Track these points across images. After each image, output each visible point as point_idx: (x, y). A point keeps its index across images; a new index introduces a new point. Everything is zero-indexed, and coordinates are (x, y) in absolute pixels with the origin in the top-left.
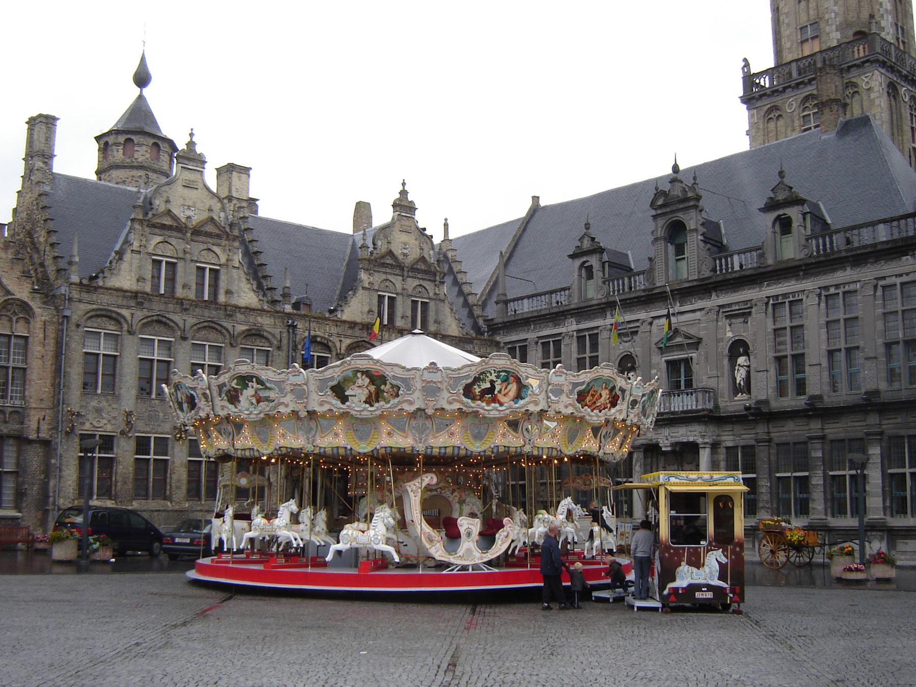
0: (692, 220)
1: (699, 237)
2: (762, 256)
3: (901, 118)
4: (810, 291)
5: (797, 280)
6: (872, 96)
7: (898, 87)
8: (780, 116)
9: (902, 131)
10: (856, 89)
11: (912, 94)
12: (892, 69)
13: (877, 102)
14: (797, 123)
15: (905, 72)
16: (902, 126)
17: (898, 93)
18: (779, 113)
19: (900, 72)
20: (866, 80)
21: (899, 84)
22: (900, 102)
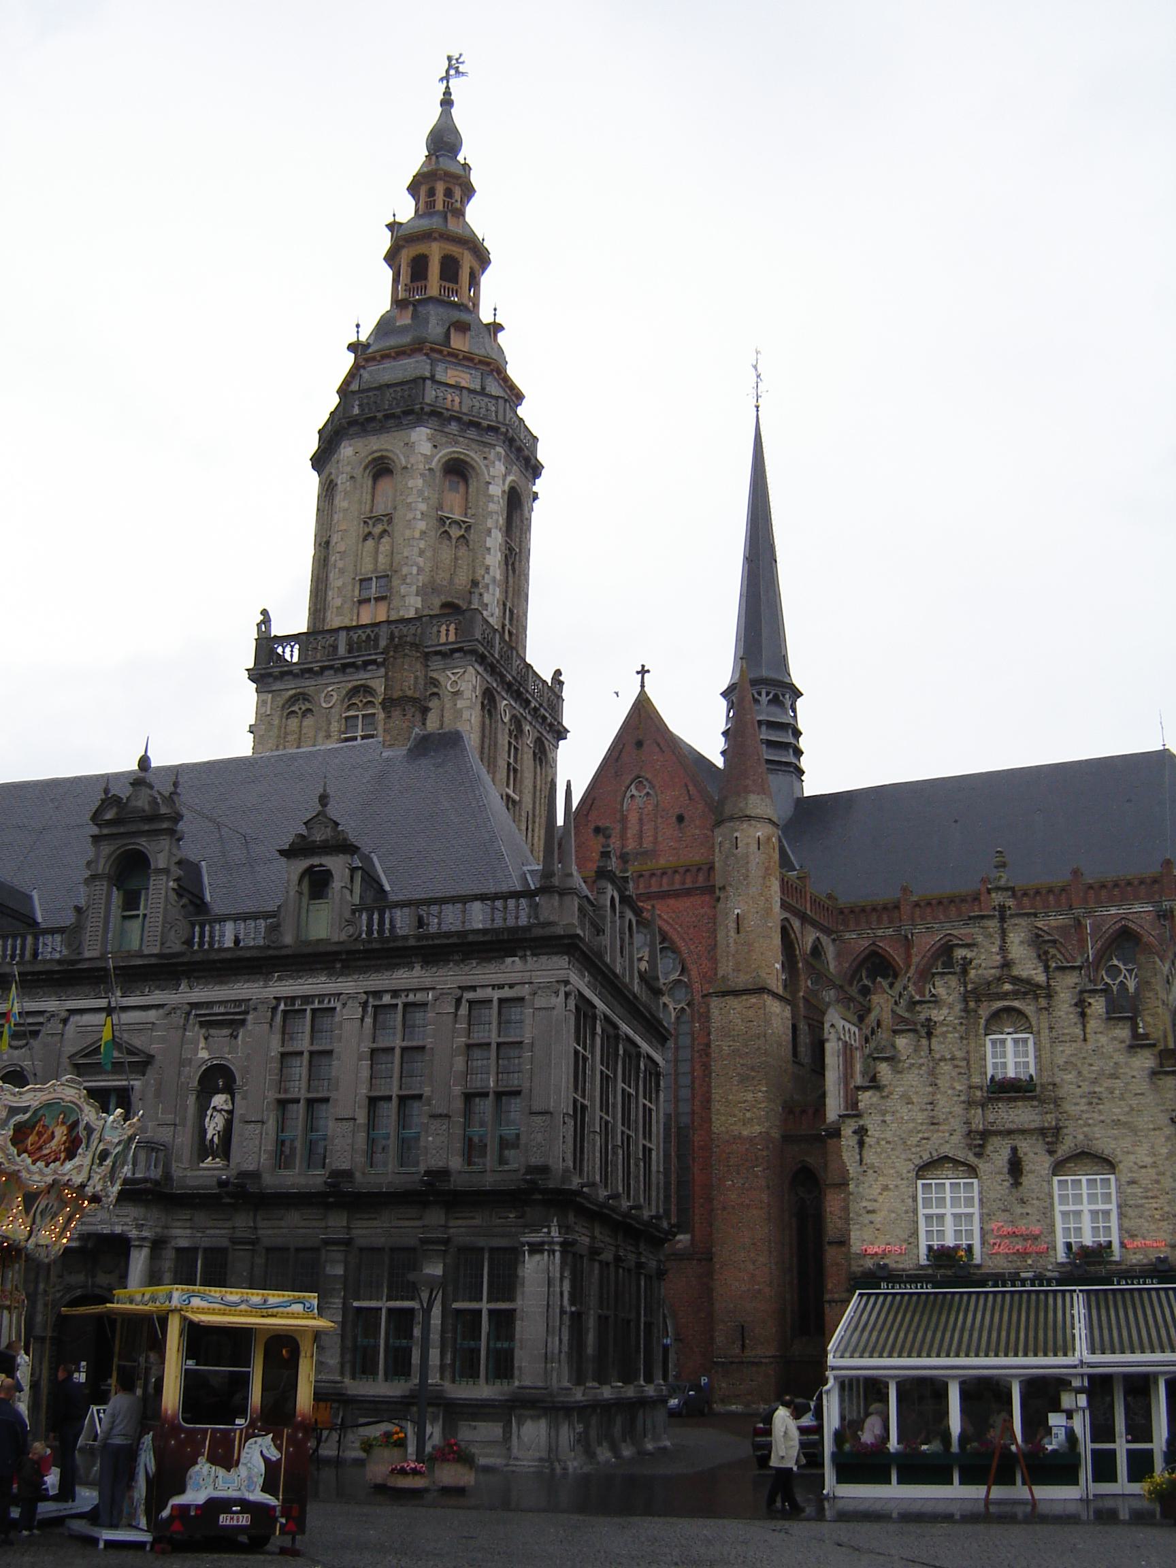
0: (160, 855)
1: (171, 884)
2: (274, 929)
3: (495, 745)
4: (351, 997)
5: (329, 975)
6: (460, 704)
7: (497, 698)
8: (309, 710)
9: (495, 766)
10: (435, 690)
11: (515, 712)
12: (492, 669)
13: (466, 715)
14: (335, 727)
15: (509, 678)
16: (495, 758)
17: (495, 708)
18: (308, 705)
19: (502, 676)
20: (453, 678)
21: (498, 693)
22: (496, 722)
